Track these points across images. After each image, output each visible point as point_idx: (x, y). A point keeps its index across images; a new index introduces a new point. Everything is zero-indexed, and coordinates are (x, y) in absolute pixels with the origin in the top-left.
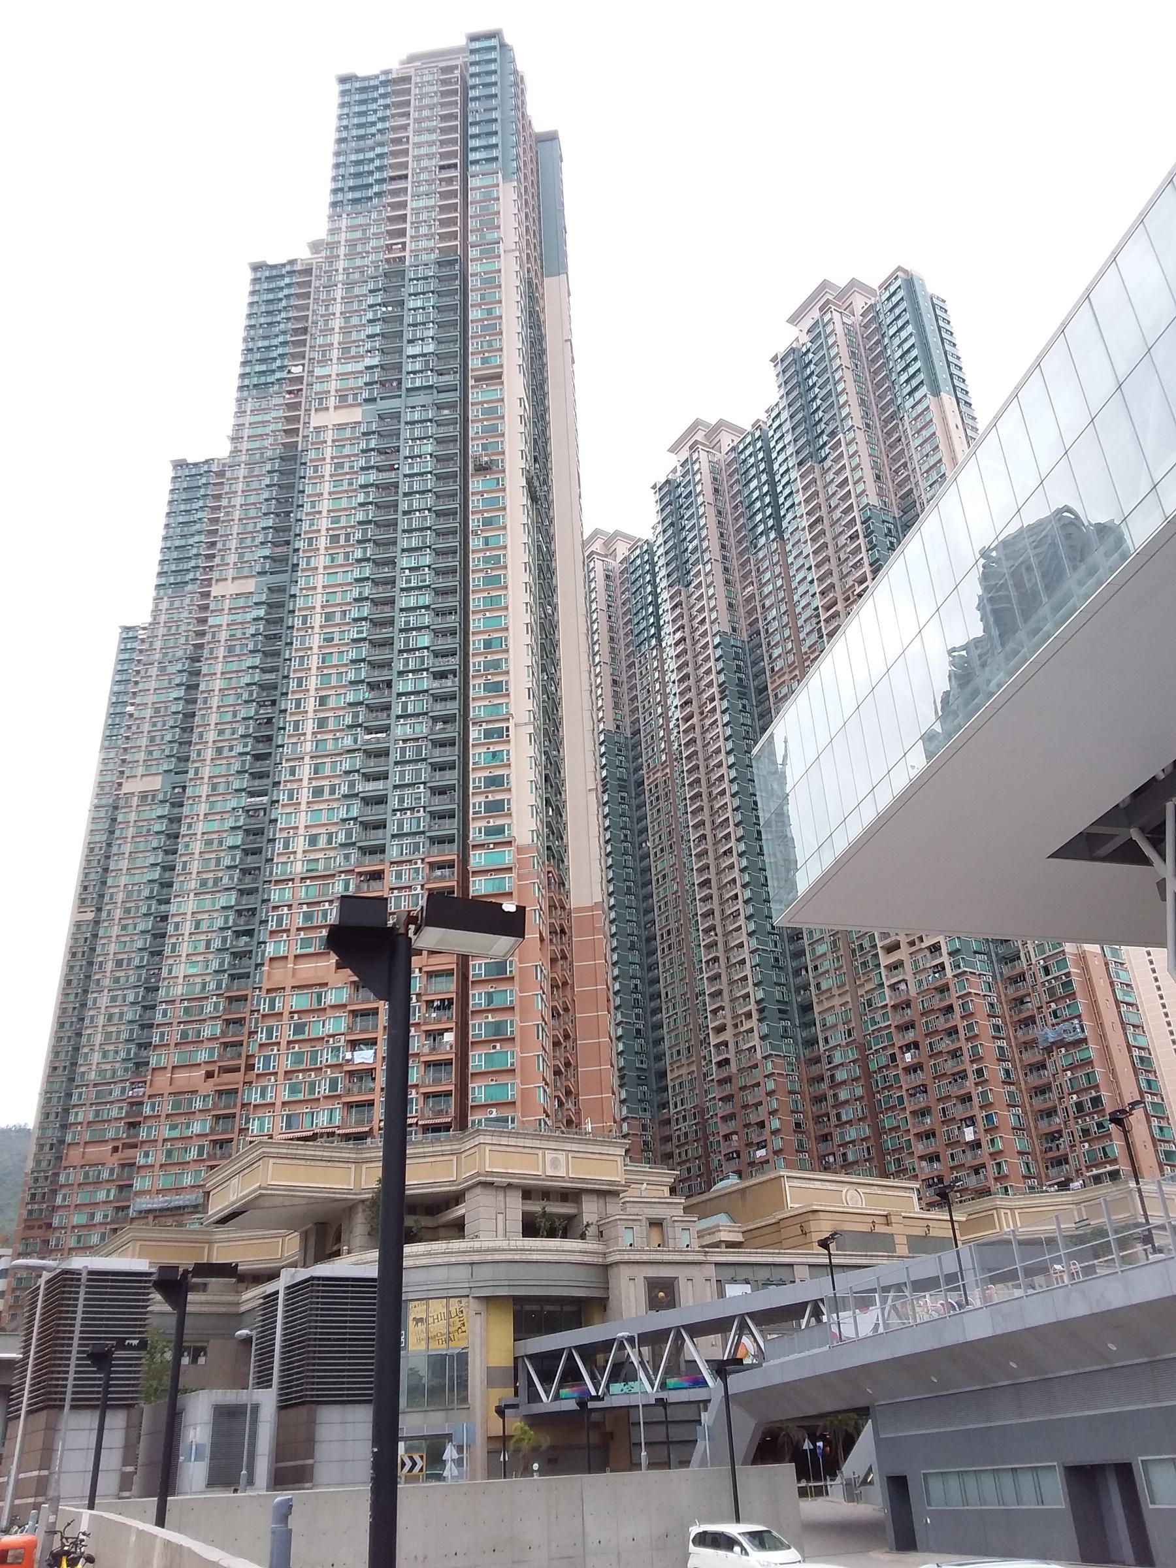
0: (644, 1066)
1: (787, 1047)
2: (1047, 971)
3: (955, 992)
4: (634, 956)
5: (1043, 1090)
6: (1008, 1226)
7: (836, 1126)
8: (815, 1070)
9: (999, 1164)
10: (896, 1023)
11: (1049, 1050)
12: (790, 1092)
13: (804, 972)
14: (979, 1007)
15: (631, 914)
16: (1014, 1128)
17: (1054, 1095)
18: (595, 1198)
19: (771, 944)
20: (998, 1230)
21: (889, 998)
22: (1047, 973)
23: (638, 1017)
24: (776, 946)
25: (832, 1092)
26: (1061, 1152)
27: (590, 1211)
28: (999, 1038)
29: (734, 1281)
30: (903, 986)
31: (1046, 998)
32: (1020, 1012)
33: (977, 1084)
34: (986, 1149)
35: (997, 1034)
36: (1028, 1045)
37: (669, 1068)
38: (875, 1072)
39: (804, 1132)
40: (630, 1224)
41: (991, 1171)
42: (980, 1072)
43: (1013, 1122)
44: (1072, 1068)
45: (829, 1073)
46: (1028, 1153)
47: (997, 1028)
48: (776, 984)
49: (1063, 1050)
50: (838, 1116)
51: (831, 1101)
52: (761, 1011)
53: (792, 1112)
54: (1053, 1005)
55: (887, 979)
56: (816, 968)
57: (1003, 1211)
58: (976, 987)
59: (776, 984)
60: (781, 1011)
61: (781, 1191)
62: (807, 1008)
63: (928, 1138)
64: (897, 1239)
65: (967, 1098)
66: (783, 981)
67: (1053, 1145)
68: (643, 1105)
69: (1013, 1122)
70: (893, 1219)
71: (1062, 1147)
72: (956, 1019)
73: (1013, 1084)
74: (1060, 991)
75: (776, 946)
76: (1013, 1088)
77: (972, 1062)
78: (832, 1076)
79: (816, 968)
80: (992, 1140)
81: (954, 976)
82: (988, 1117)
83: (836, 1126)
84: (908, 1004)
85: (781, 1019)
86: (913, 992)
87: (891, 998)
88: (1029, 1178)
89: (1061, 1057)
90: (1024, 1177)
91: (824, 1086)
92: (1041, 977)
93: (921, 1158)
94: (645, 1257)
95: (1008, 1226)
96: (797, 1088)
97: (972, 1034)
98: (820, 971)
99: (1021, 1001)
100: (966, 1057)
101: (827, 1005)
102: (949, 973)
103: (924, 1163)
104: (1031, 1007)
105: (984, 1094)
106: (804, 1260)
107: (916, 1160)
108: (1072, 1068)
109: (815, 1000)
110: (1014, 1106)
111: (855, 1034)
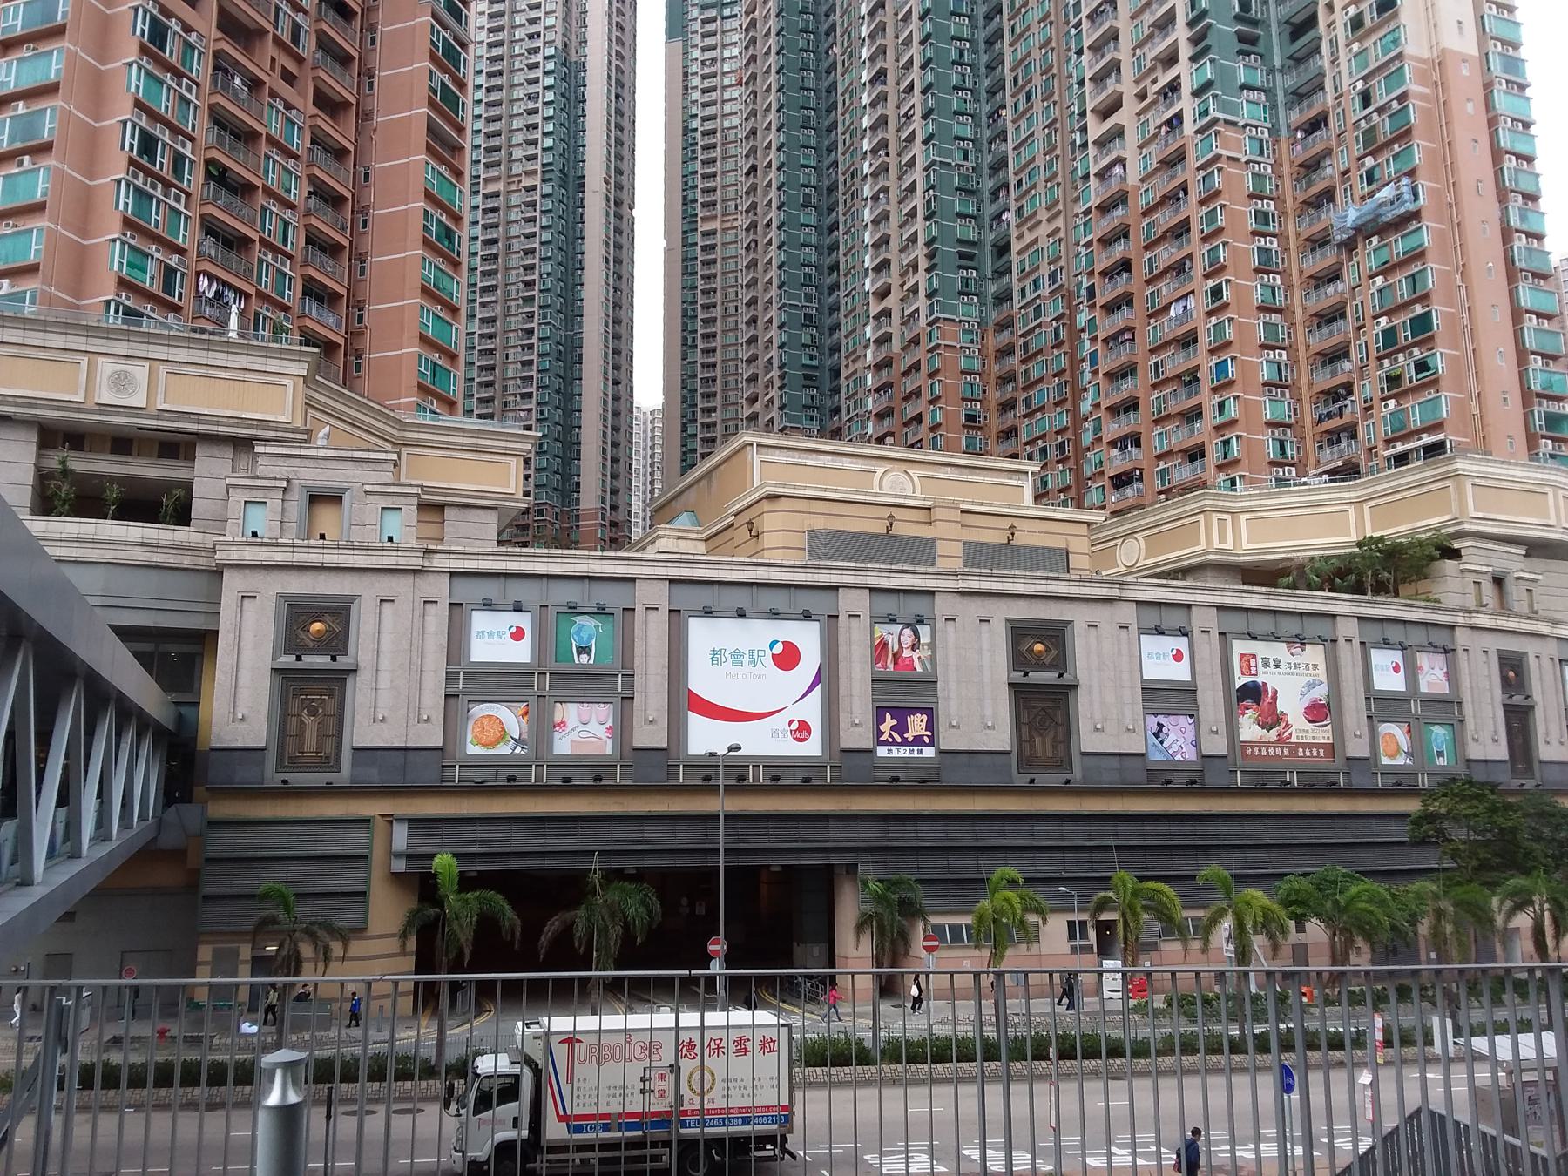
0: (814, 363)
1: (966, 309)
2: (1366, 99)
3: (1194, 159)
4: (810, 217)
5: (1333, 315)
6: (1223, 539)
7: (1025, 416)
8: (1005, 337)
9: (1226, 443)
10: (1100, 234)
11: (1349, 246)
12: (963, 373)
13: (1002, 193)
15: (806, 157)
16: (1264, 385)
17: (1346, 327)
18: (228, 452)
19: (958, 157)
20: (1203, 546)
21: (1095, 194)
22: (1366, 99)
23: (808, 297)
24: (966, 158)
25: (1024, 367)
26: (1346, 419)
27: (209, 476)
28: (1264, 235)
29: (488, 605)
30: (1117, 170)
31: (1359, 149)
32: (1309, 185)
33: (1210, 314)
34: (1210, 419)
35: (1263, 228)
36: (1318, 242)
37: (844, 363)
38: (1082, 330)
39: (980, 428)
40: (259, 496)
41: (1214, 454)
42: (1216, 292)
43: (1266, 373)
44: (1387, 270)
45: (1022, 340)
46: (1289, 426)
47: (1263, 217)
48: (960, 215)
49: (1375, 240)
50: (1028, 401)
51: (1021, 381)
52: (930, 256)
53: (964, 399)
54: (1369, 162)
55: (1096, 162)
56: (1020, 183)
57: (1215, 517)
59: (960, 215)
60: (962, 256)
61: (746, 468)
62: (1003, 249)
63: (1127, 410)
64: (940, 548)
65: (1188, 341)
67: (1333, 408)
68: (809, 412)
69: (1266, 373)
70: (938, 514)
71: (1347, 411)
72: (1191, 209)
73: (1278, 311)
74: (1386, 131)
75: (966, 158)
76: (1275, 318)
77: (1207, 277)
78: (1026, 345)
79: (1020, 183)
80: (1221, 406)
81: (1196, 132)
82: (1221, 366)
83: (1025, 416)
84: (1120, 199)
85: (960, 267)
86: (1134, 175)
87: (1097, 195)
88: (1282, 465)
89: (1370, 255)
90: (1272, 463)
91: (1012, 361)
92: (1356, 112)
93: (1113, 444)
94: (279, 557)
95: (1223, 539)
96: (976, 365)
97: (1213, 228)
98: (1024, 187)
99: (1311, 166)
100: (1198, 270)
101: (1028, 238)
102: (1189, 127)
103: (1115, 452)
104: (1330, 171)
105: (1219, 327)
106: (661, 571)
107: (1104, 447)
108: (1387, 270)
109: (1014, 233)
110: (1273, 348)
111: (1063, 278)
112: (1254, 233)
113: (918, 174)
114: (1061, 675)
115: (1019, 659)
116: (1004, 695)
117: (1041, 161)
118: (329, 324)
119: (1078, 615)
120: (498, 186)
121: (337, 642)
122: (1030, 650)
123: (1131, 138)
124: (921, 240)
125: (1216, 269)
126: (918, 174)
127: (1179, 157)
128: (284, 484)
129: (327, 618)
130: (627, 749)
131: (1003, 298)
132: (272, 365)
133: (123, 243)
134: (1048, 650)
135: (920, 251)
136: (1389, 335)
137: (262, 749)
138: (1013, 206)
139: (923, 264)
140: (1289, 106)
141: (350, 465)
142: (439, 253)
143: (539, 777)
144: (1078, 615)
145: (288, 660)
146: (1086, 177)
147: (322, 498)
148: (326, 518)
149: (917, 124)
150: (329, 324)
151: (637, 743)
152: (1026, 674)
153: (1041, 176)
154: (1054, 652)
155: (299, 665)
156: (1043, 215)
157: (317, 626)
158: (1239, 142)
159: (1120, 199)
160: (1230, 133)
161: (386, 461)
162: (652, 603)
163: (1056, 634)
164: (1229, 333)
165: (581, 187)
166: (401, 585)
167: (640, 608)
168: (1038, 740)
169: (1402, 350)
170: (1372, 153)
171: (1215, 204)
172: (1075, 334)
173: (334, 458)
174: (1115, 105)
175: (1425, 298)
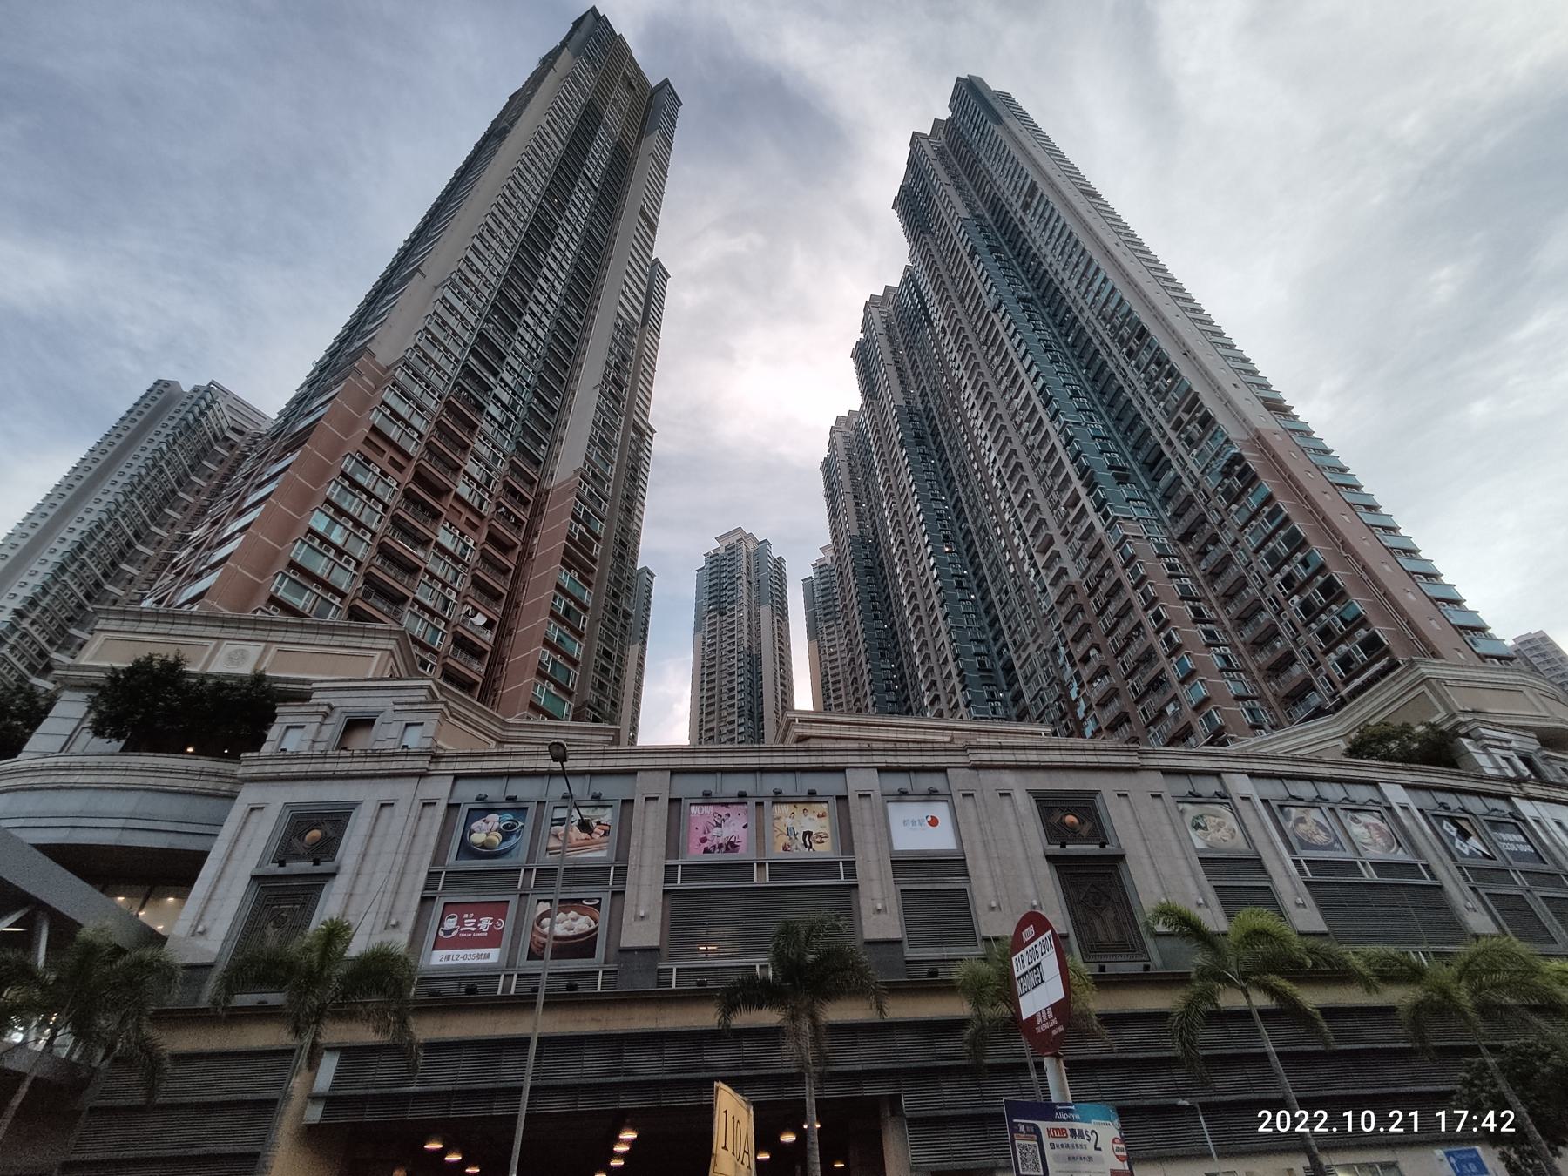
3: (1109, 546)
9: (1209, 717)
14: (1146, 552)
16: (1221, 670)
21: (1053, 594)
28: (1179, 577)
33: (1157, 632)
42: (1158, 617)
58: (1130, 529)
62: (1009, 668)
66: (983, 650)
69: (1219, 663)
77: (1146, 609)
101: (1024, 656)
102: (1100, 529)
109: (1014, 657)
112: (1170, 577)
113: (944, 637)
114: (1103, 845)
115: (1055, 832)
116: (1045, 870)
117: (1019, 610)
118: (476, 670)
119: (1105, 785)
120: (714, 724)
121: (327, 848)
122: (1063, 824)
123: (1066, 556)
124: (954, 674)
125: (1151, 602)
126: (944, 637)
127: (1100, 546)
128: (325, 709)
129: (328, 826)
130: (613, 951)
131: (1018, 696)
132: (366, 643)
133: (285, 576)
134: (1081, 822)
135: (955, 680)
136: (1306, 607)
137: (210, 966)
138: (1009, 642)
139: (958, 687)
140: (1164, 508)
141: (390, 693)
142: (563, 623)
143: (506, 988)
144: (1105, 785)
145: (274, 869)
146: (1044, 590)
147: (358, 723)
148: (360, 741)
149: (934, 598)
150: (476, 670)
151: (625, 944)
152: (1063, 846)
153: (1021, 618)
154: (1088, 826)
155: (281, 871)
156: (1029, 640)
157: (316, 833)
158: (1141, 530)
159: (1071, 589)
160: (1128, 524)
161: (421, 687)
162: (652, 792)
163: (1085, 804)
164: (1176, 639)
165: (761, 719)
166: (403, 791)
167: (639, 801)
168: (1097, 923)
169: (1322, 611)
170: (1235, 502)
171: (1135, 563)
172: (1073, 705)
173: (378, 688)
174: (1051, 541)
175: (1322, 568)
